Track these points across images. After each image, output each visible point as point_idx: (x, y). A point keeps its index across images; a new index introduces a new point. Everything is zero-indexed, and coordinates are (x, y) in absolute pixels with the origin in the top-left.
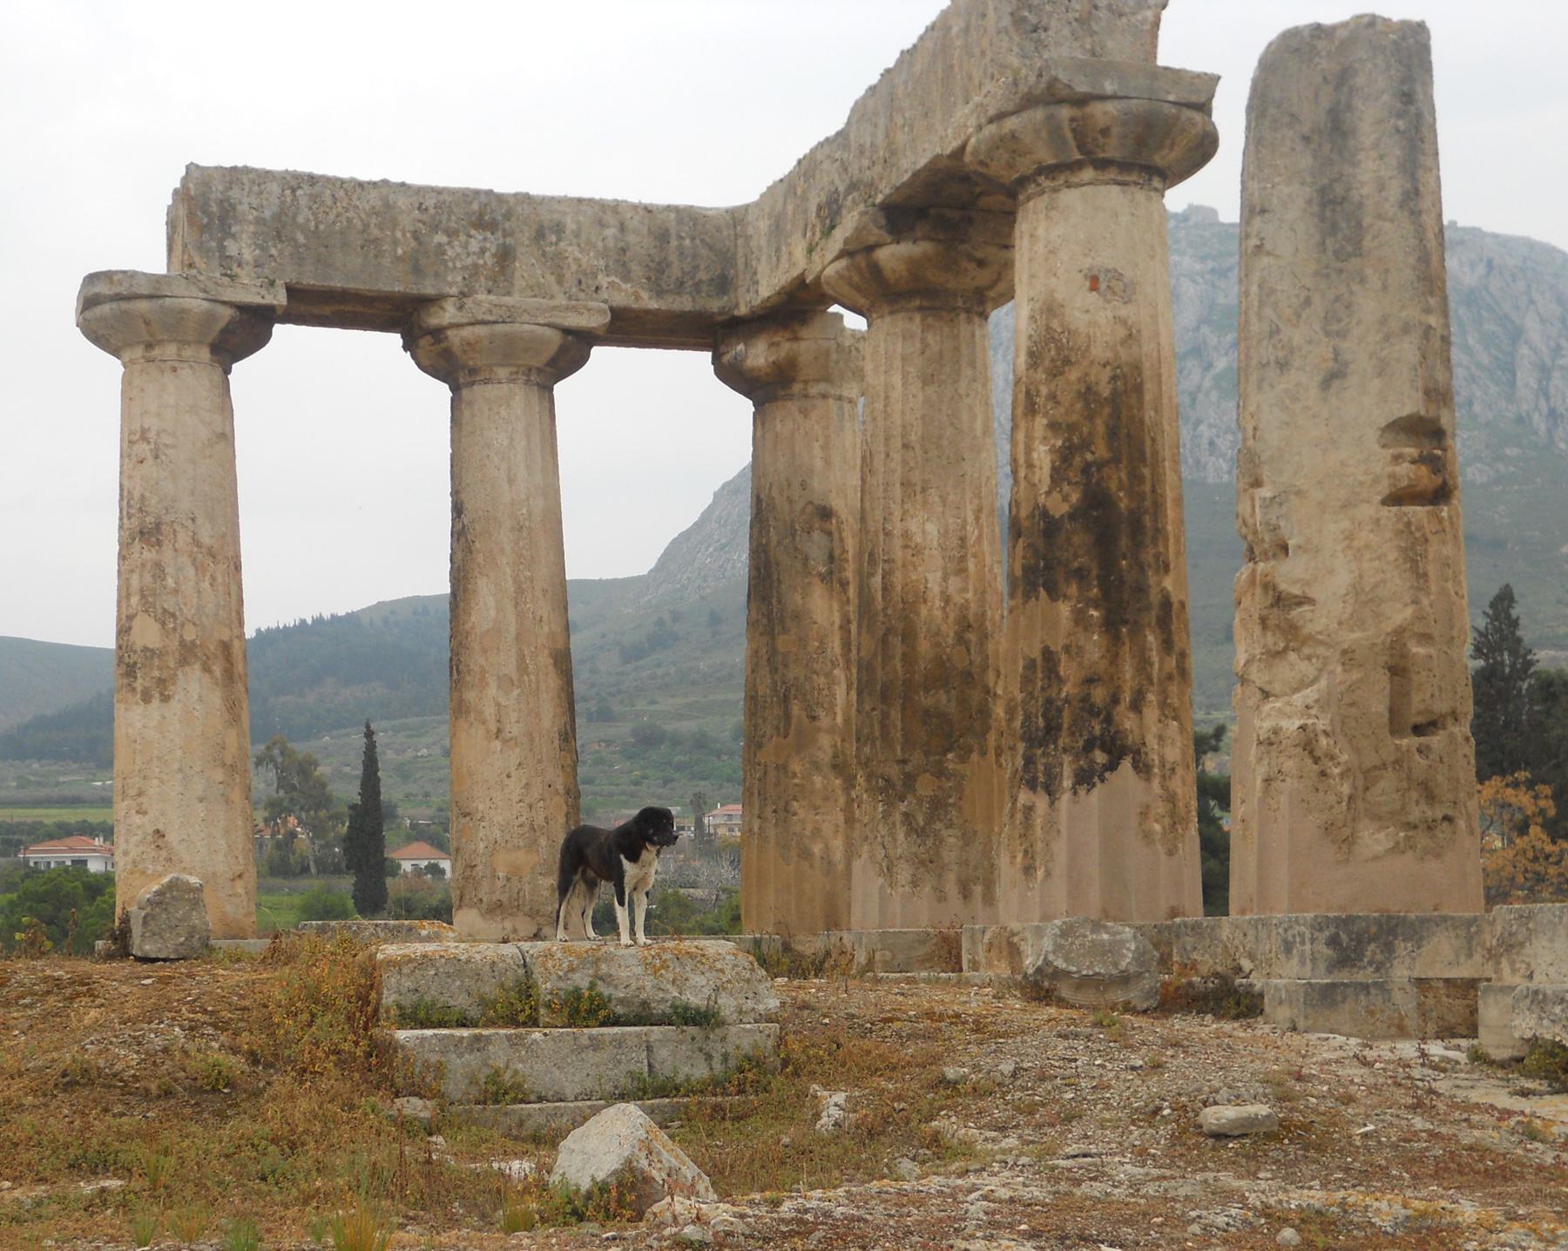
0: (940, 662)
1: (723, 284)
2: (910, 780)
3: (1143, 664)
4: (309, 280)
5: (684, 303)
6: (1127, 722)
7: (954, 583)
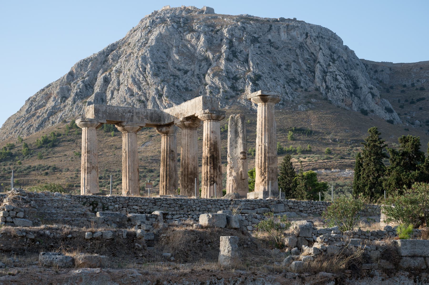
0: (191, 172)
1: (160, 121)
2: (188, 186)
3: (217, 173)
4: (108, 120)
5: (155, 123)
6: (215, 178)
7: (193, 162)
